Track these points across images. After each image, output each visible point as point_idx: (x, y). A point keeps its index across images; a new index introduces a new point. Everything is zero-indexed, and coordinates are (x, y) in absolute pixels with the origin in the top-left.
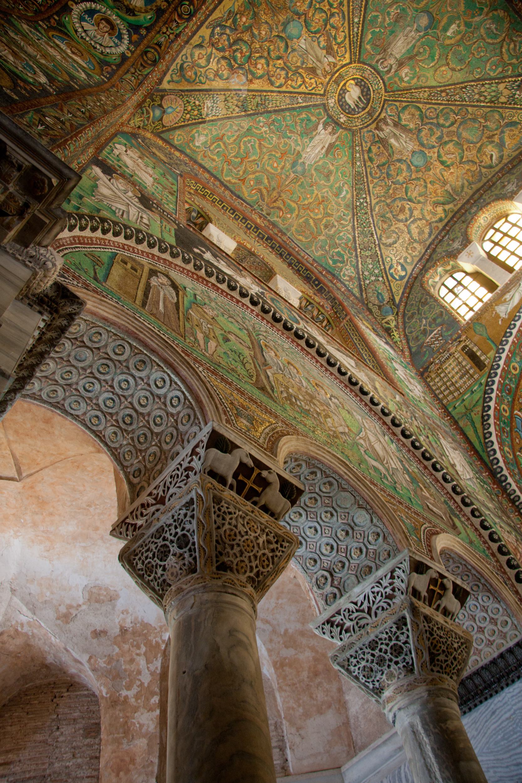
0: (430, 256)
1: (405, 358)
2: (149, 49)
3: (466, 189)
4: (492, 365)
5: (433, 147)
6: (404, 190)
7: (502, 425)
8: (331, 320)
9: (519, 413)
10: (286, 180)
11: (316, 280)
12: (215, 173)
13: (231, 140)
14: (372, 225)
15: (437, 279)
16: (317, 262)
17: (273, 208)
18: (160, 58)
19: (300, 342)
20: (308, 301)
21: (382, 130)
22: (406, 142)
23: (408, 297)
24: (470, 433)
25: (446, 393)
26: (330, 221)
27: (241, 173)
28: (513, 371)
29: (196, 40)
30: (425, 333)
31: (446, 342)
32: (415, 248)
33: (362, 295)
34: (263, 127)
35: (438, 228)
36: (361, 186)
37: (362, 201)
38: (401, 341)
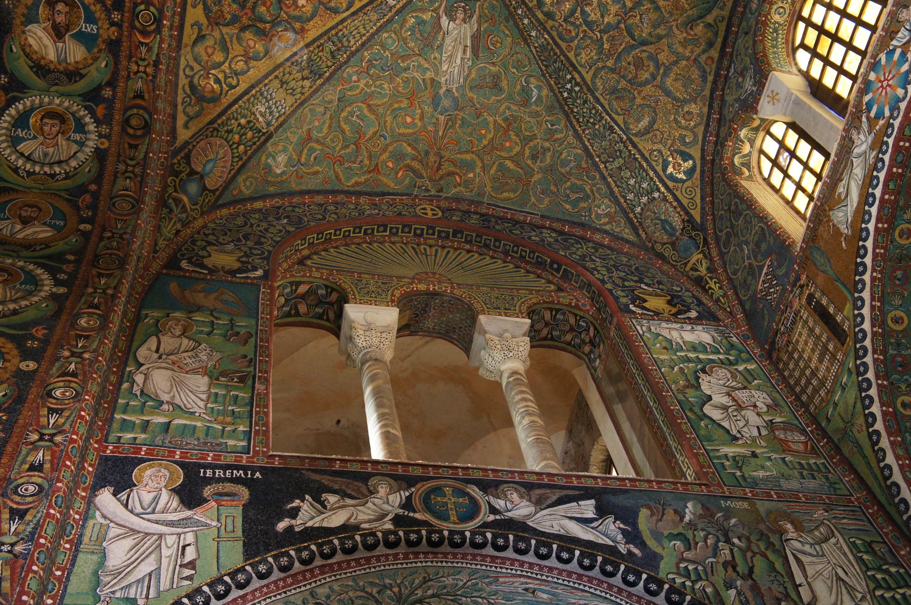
0: (720, 113)
1: (739, 327)
2: (129, 113)
8: (598, 327)
11: (553, 262)
12: (328, 187)
13: (325, 130)
14: (604, 114)
15: (746, 149)
16: (548, 218)
17: (441, 178)
18: (151, 116)
19: (483, 552)
20: (551, 310)
23: (712, 202)
24: (862, 469)
25: (809, 390)
26: (535, 146)
27: (366, 162)
29: (190, 34)
30: (753, 272)
31: (784, 290)
32: (688, 113)
33: (638, 235)
34: (359, 81)
35: (712, 58)
36: (557, 65)
37: (569, 86)
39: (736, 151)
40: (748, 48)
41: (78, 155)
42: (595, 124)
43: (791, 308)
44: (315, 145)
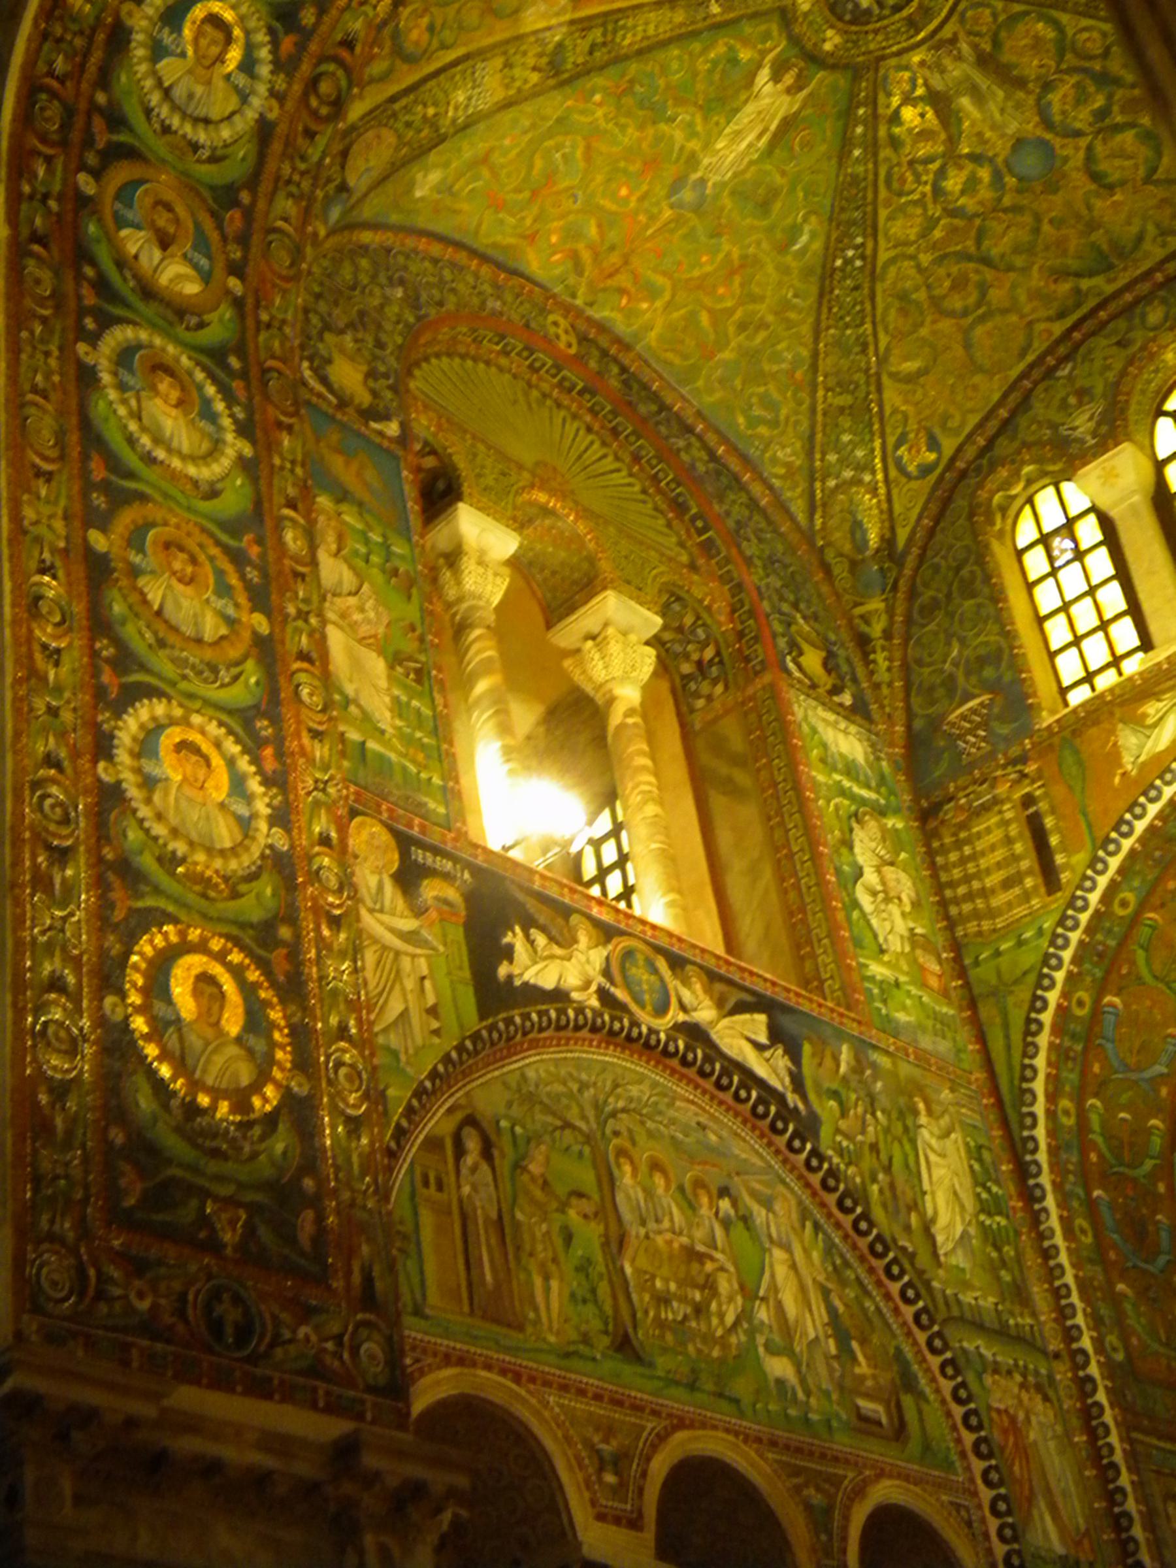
0: (1014, 413)
1: (892, 745)
3: (1147, 245)
4: (1074, 898)
5: (1078, 134)
6: (973, 233)
7: (1067, 1043)
9: (1116, 1000)
10: (647, 227)
12: (457, 237)
15: (1017, 489)
17: (605, 290)
18: (350, 86)
19: (668, 1061)
21: (942, 71)
22: (1002, 111)
23: (931, 532)
27: (528, 222)
28: (1121, 912)
31: (992, 755)
32: (975, 388)
35: (1050, 333)
37: (850, 253)
38: (890, 684)
39: (1007, 485)
40: (1108, 368)
41: (237, 118)
42: (847, 326)
43: (993, 787)
44: (485, 172)
